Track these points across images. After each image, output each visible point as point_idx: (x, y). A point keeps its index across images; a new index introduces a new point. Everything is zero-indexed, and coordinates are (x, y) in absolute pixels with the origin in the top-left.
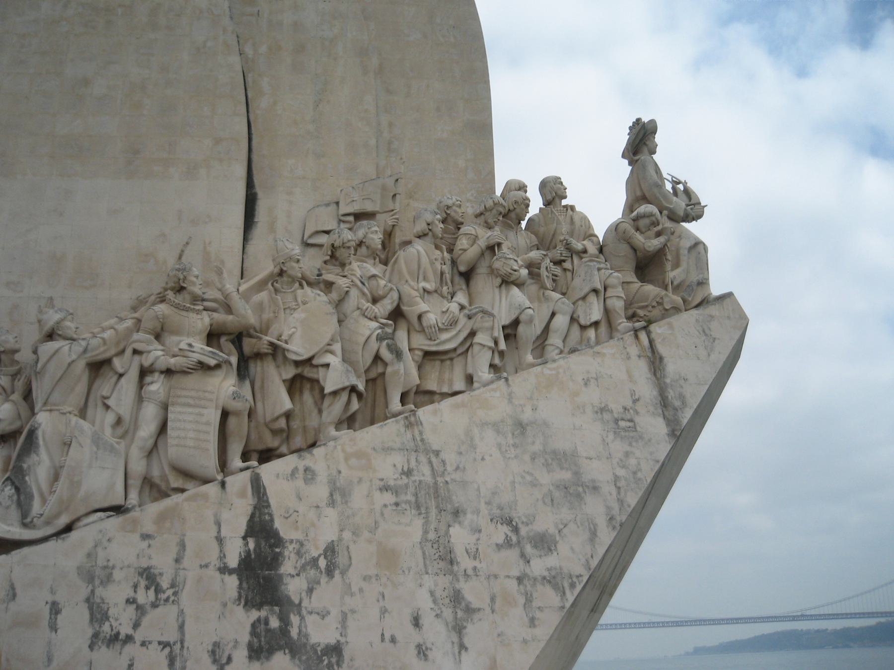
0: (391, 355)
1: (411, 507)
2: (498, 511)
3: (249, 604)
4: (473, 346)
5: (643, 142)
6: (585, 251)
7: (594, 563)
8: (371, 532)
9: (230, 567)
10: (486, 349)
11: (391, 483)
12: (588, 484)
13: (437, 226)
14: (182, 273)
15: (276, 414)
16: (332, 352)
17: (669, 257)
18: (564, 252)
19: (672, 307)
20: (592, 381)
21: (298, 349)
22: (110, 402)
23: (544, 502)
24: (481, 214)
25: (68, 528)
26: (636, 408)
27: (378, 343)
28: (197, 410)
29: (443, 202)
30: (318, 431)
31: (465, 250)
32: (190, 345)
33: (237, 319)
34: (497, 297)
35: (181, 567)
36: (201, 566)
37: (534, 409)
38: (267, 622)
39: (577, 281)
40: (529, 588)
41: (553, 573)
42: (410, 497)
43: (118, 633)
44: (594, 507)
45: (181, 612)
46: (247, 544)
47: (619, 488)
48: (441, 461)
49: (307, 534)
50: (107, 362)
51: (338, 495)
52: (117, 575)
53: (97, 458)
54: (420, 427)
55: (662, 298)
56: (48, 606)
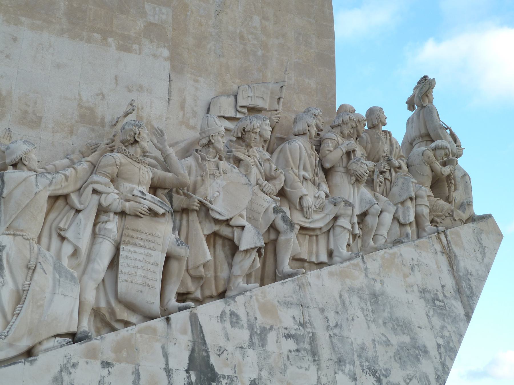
0: (285, 226)
1: (308, 354)
2: (367, 364)
4: (334, 228)
5: (426, 94)
6: (400, 168)
8: (282, 373)
10: (346, 231)
11: (293, 332)
12: (421, 348)
13: (314, 128)
14: (138, 129)
15: (198, 263)
16: (241, 216)
18: (386, 166)
19: (459, 219)
20: (416, 267)
22: (68, 235)
23: (396, 361)
24: (339, 125)
26: (444, 292)
27: (275, 214)
28: (147, 251)
29: (311, 111)
30: (229, 280)
31: (331, 151)
32: (142, 193)
33: (177, 177)
34: (352, 192)
37: (382, 283)
39: (395, 190)
42: (307, 346)
46: (189, 377)
47: (440, 354)
48: (325, 318)
49: (235, 371)
50: (66, 197)
51: (256, 338)
53: (59, 285)
54: (309, 287)
55: (452, 211)
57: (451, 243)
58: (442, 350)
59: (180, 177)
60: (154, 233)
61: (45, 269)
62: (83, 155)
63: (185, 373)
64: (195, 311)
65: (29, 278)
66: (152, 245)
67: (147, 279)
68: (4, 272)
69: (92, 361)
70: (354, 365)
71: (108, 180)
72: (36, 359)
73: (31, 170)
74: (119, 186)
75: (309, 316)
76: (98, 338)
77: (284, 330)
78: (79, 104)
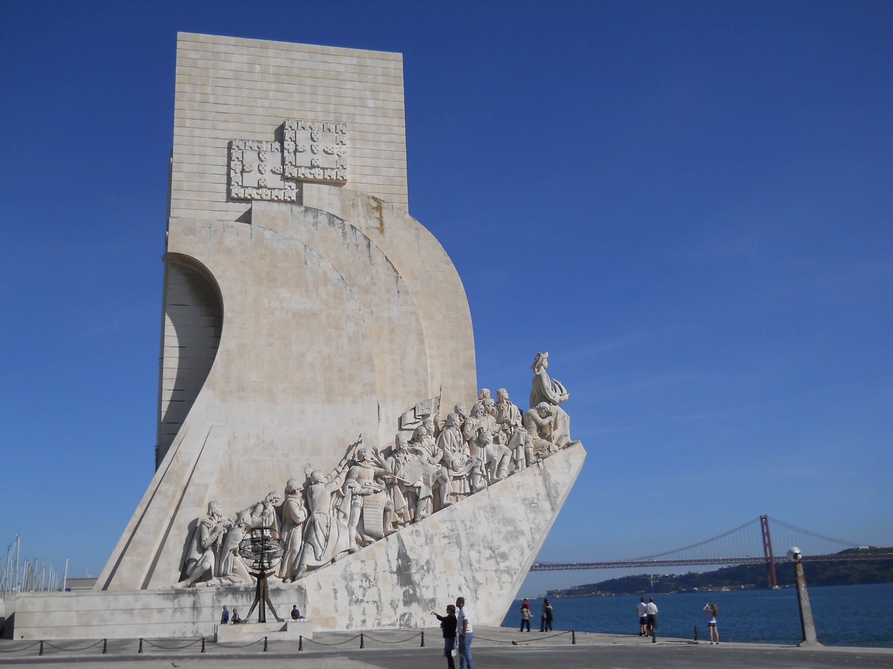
2: (487, 544)
3: (402, 585)
6: (516, 425)
7: (523, 564)
11: (447, 535)
17: (553, 426)
21: (408, 480)
23: (504, 540)
25: (333, 561)
28: (375, 510)
32: (370, 483)
36: (383, 572)
38: (408, 591)
40: (499, 575)
41: (508, 568)
43: (358, 599)
44: (523, 541)
45: (379, 589)
47: (532, 533)
50: (338, 491)
52: (355, 577)
55: (549, 447)
56: (333, 591)
57: (547, 467)
58: (533, 530)
59: (387, 470)
64: (399, 533)
66: (376, 506)
70: (479, 546)
73: (321, 483)
75: (456, 525)
77: (442, 535)
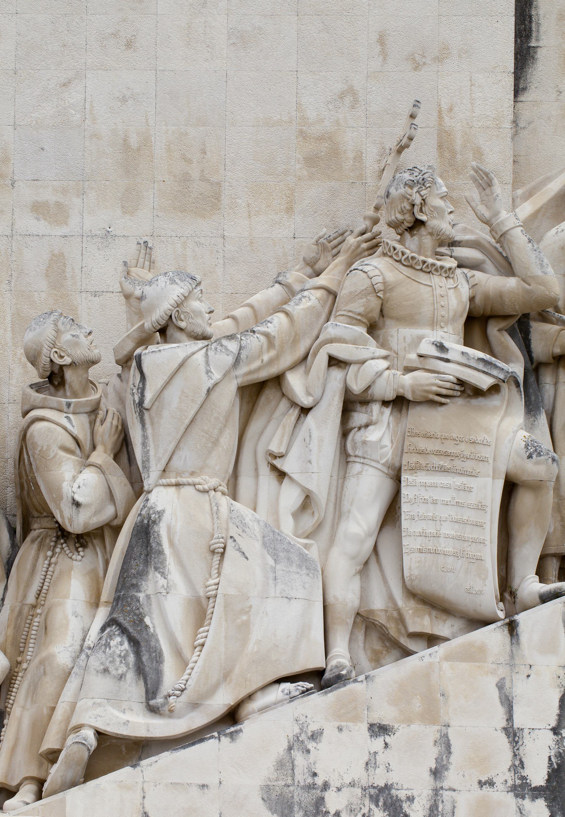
9: (532, 786)
28: (459, 481)
35: (446, 785)
36: (481, 784)
53: (275, 579)
60: (473, 437)
61: (244, 550)
62: (312, 267)
63: (551, 733)
65: (216, 571)
66: (468, 465)
67: (465, 542)
68: (166, 566)
69: (350, 724)
71: (362, 330)
72: (241, 730)
74: (389, 338)
76: (359, 680)
78: (301, 132)
